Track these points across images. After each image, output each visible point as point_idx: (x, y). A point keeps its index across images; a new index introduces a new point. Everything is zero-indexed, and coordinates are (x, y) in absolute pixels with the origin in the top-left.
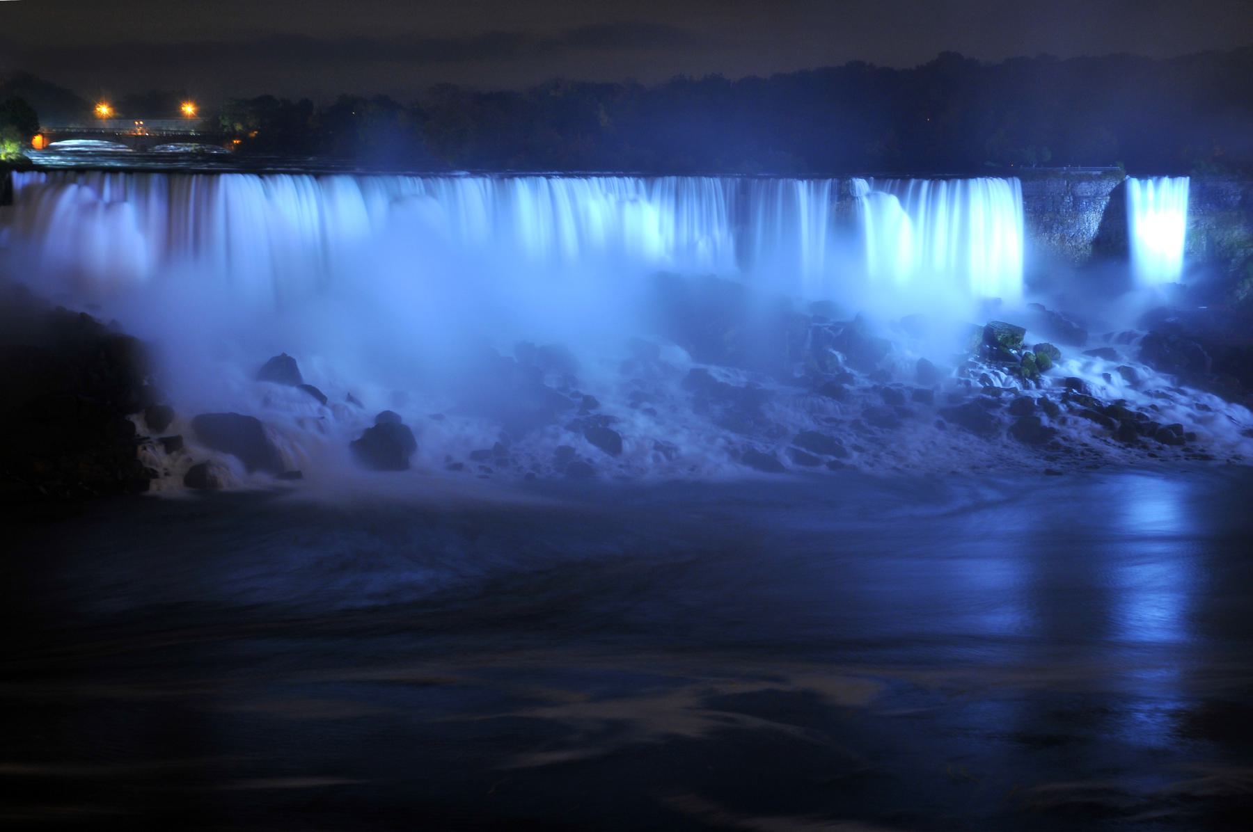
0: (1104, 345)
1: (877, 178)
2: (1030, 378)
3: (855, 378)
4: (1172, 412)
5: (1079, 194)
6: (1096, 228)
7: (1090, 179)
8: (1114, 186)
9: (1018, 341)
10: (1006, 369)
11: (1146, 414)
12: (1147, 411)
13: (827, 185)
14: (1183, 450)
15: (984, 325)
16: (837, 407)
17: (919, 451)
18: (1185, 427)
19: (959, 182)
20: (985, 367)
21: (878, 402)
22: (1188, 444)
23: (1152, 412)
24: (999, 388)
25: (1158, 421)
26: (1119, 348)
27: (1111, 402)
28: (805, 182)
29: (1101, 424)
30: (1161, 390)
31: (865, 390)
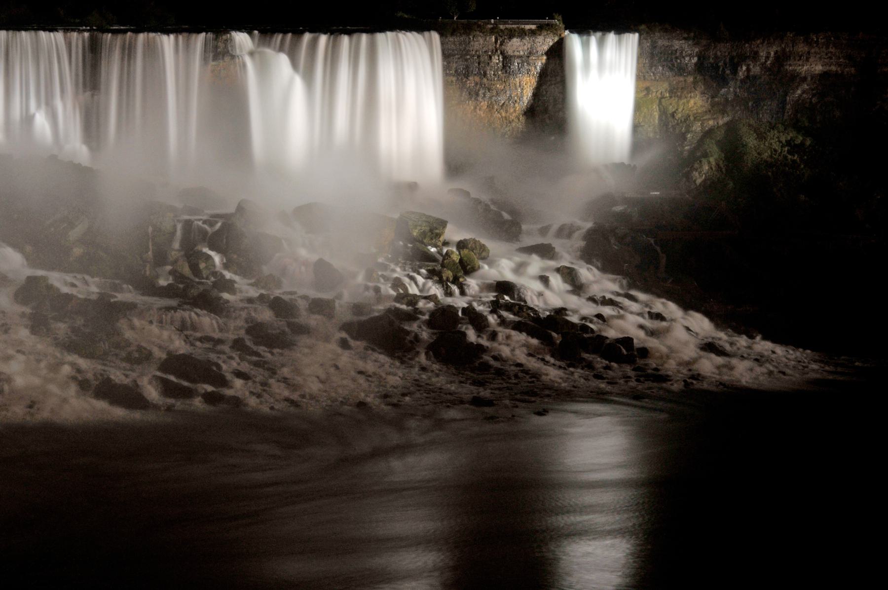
0: (538, 240)
2: (453, 282)
3: (236, 285)
4: (620, 322)
5: (510, 53)
6: (530, 94)
7: (522, 34)
8: (551, 44)
9: (438, 235)
10: (423, 271)
11: (592, 326)
12: (591, 322)
13: (200, 40)
14: (634, 370)
15: (396, 216)
16: (214, 322)
17: (318, 377)
18: (635, 341)
19: (364, 37)
20: (398, 269)
21: (266, 315)
22: (640, 362)
23: (598, 323)
24: (415, 295)
25: (604, 334)
26: (558, 245)
27: (550, 311)
28: (172, 36)
29: (537, 338)
30: (608, 296)
31: (250, 300)
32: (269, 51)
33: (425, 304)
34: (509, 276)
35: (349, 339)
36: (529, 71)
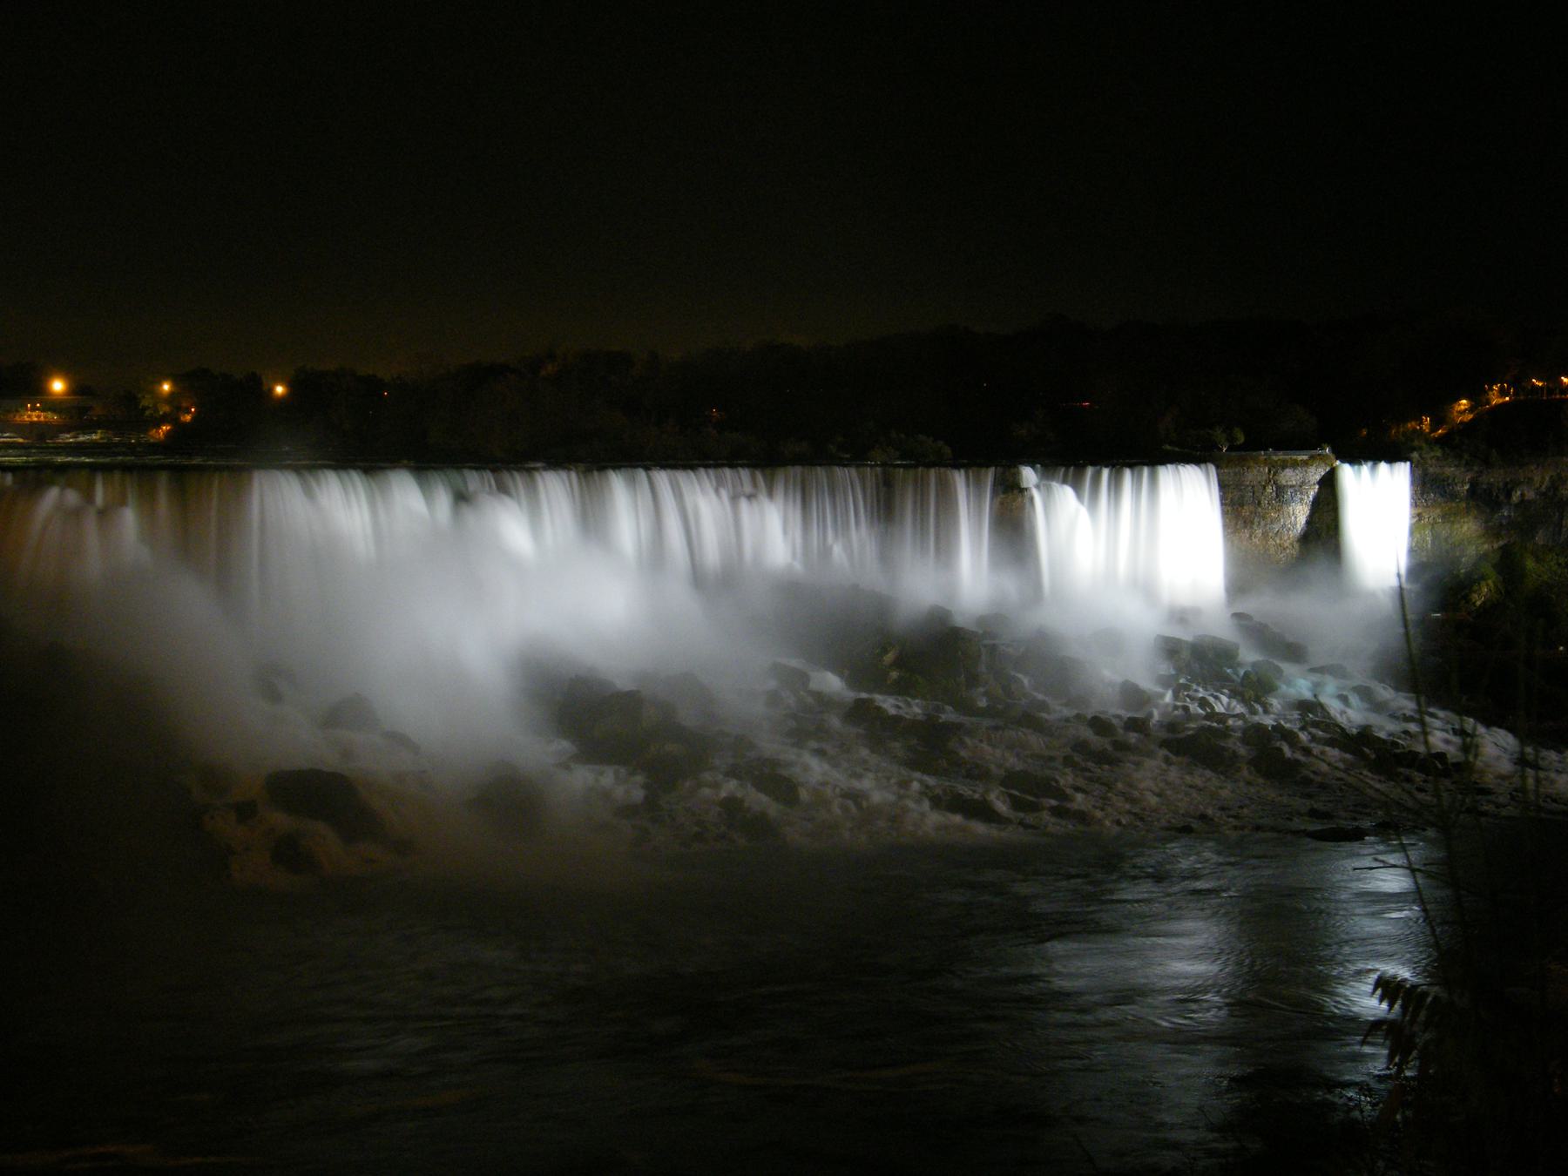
1: (1045, 466)
5: (1284, 482)
10: (1226, 691)
13: (989, 475)
20: (1201, 690)
21: (1087, 734)
23: (1406, 739)
28: (962, 471)
29: (1351, 754)
31: (1067, 720)
32: (1055, 485)
33: (1234, 722)
34: (1307, 695)
35: (1171, 755)
36: (1302, 499)
